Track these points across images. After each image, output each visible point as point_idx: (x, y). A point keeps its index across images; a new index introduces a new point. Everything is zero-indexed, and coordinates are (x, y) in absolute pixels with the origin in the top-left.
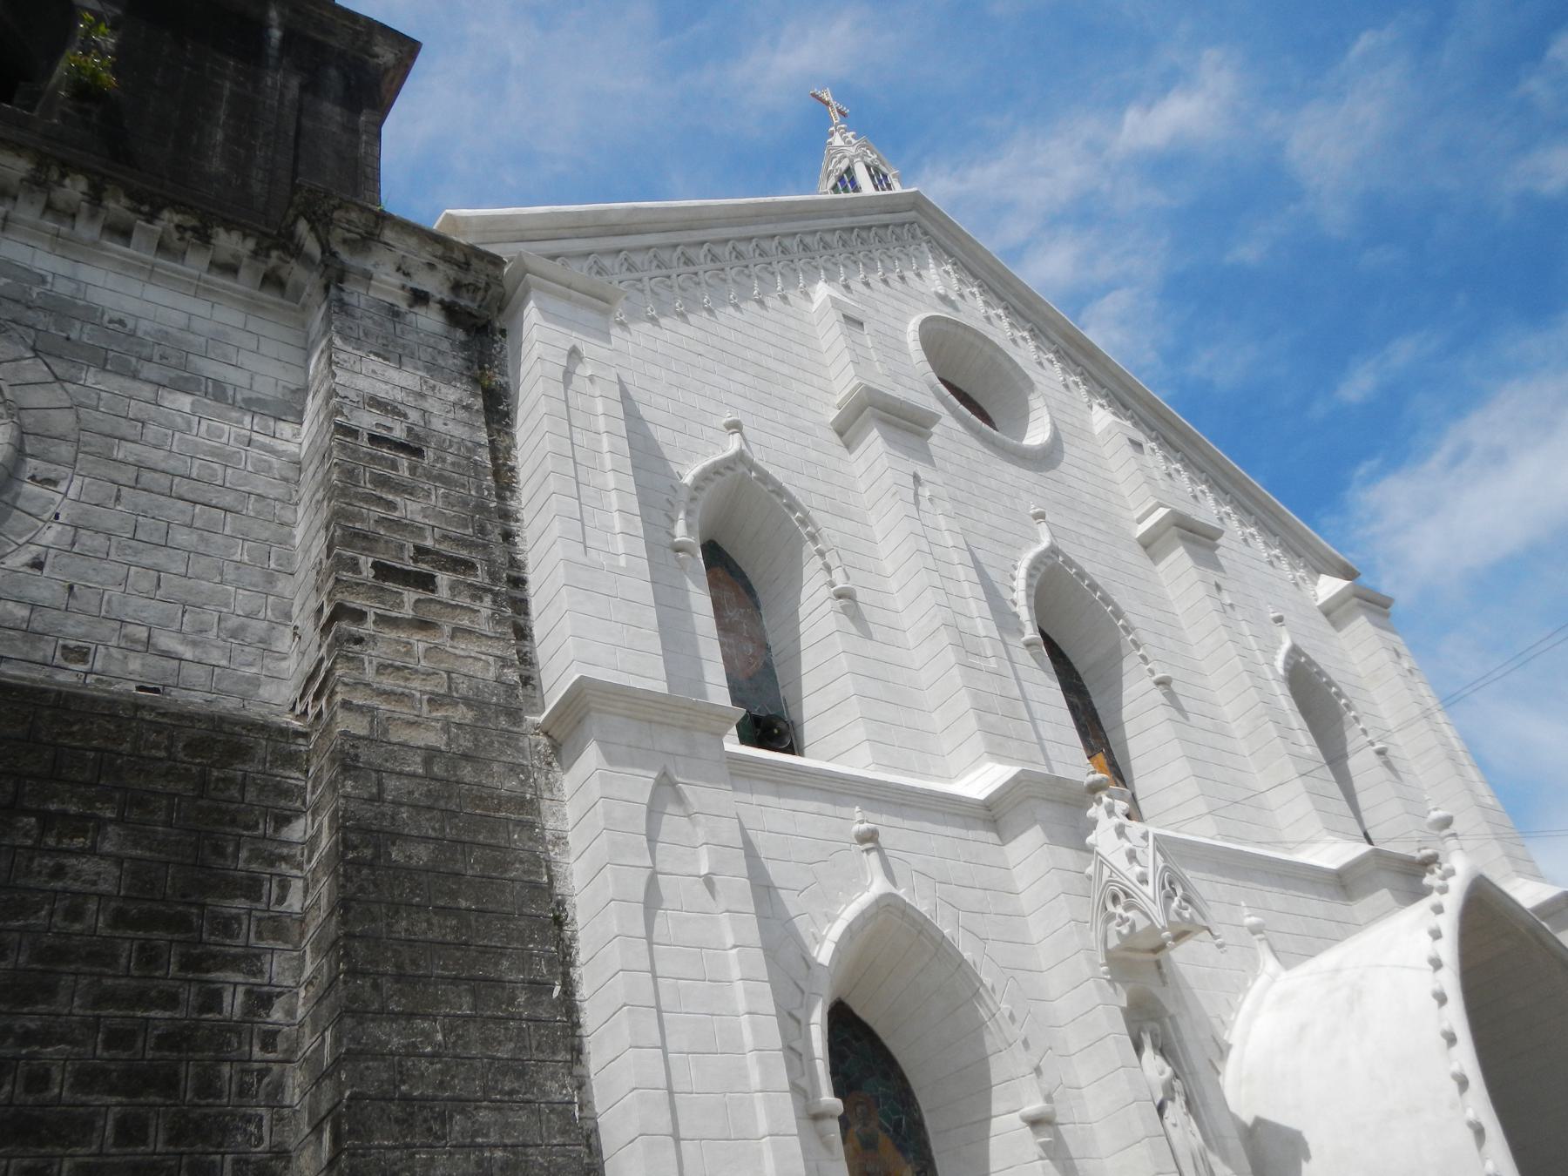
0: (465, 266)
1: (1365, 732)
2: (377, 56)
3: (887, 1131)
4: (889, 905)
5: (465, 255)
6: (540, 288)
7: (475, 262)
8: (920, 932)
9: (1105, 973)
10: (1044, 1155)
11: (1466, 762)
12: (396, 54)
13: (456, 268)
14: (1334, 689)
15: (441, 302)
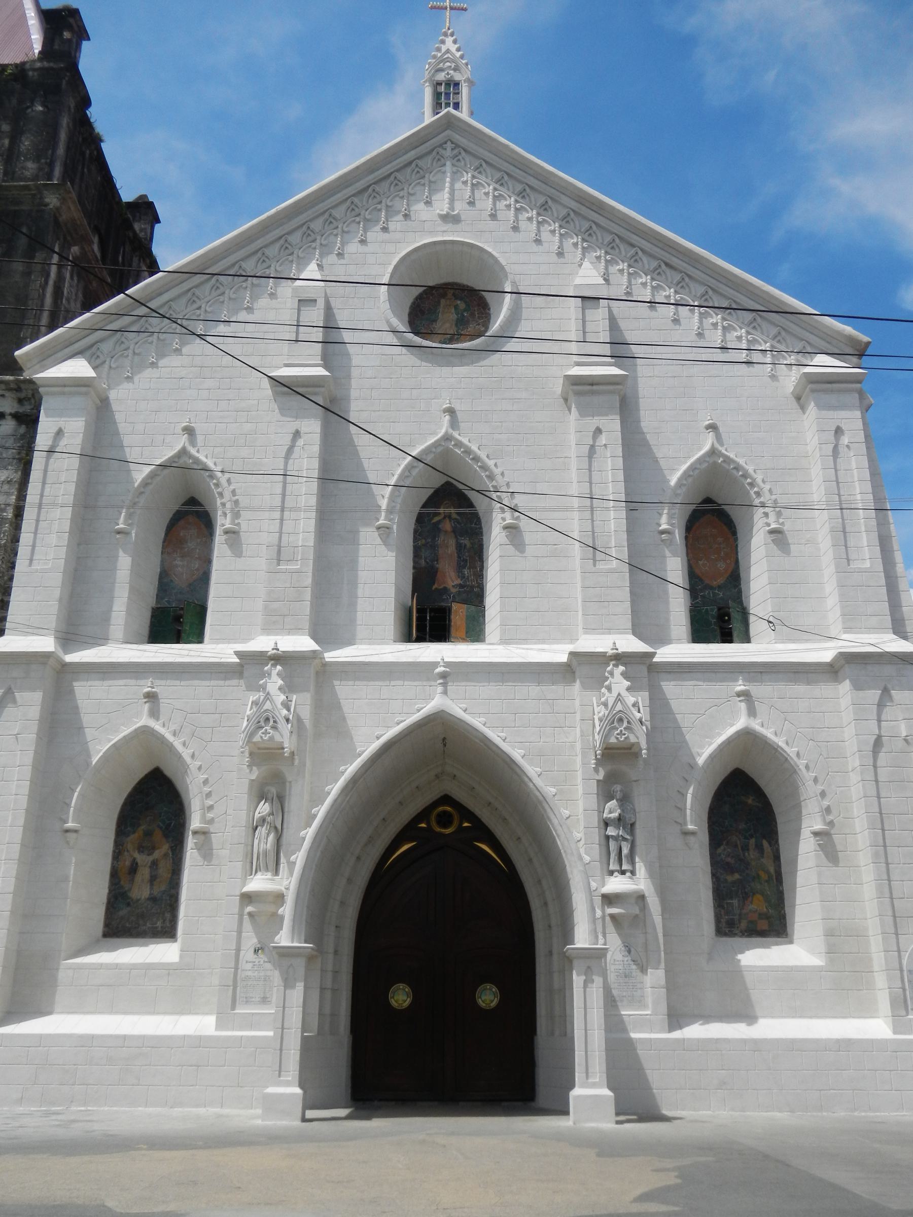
0: (19, 389)
1: (766, 515)
2: (47, 205)
3: (161, 828)
4: (144, 731)
5: (16, 384)
6: (48, 394)
7: (23, 386)
8: (162, 743)
9: (247, 762)
10: (194, 848)
12: (58, 198)
13: (15, 392)
14: (749, 480)
15: (11, 414)
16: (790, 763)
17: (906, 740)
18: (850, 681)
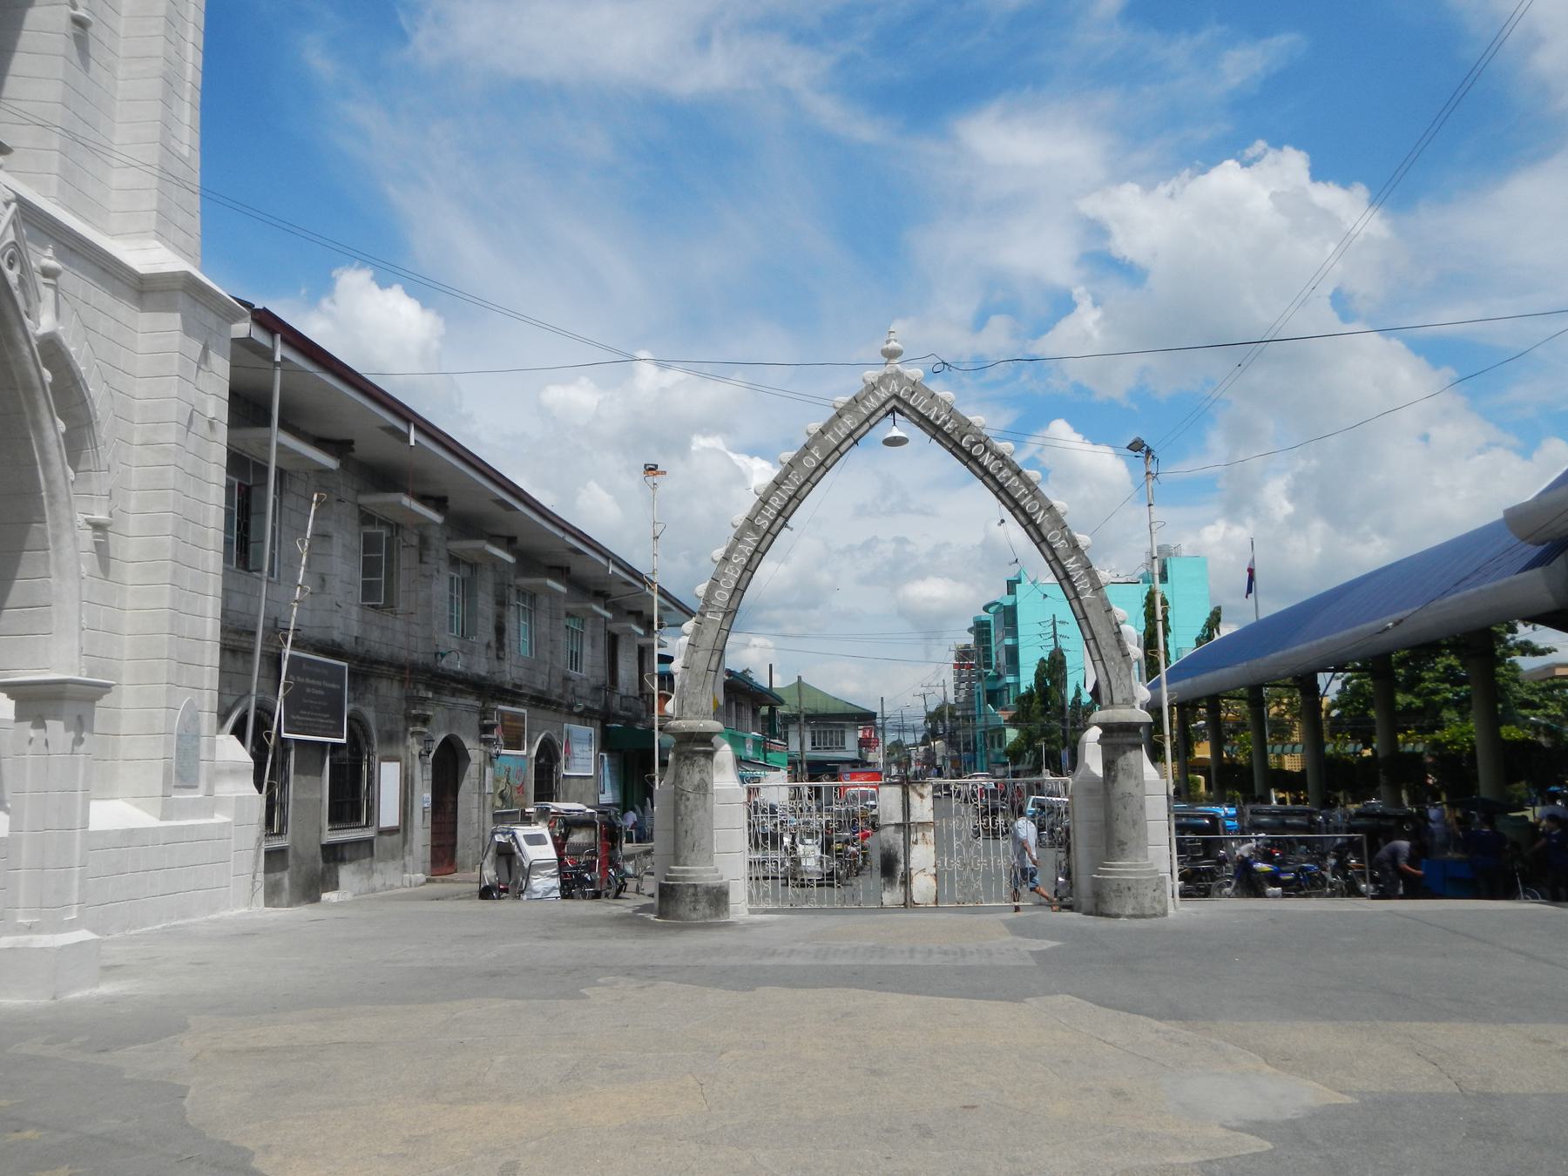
11: (187, 97)
16: (88, 408)
17: (211, 424)
18: (182, 316)
